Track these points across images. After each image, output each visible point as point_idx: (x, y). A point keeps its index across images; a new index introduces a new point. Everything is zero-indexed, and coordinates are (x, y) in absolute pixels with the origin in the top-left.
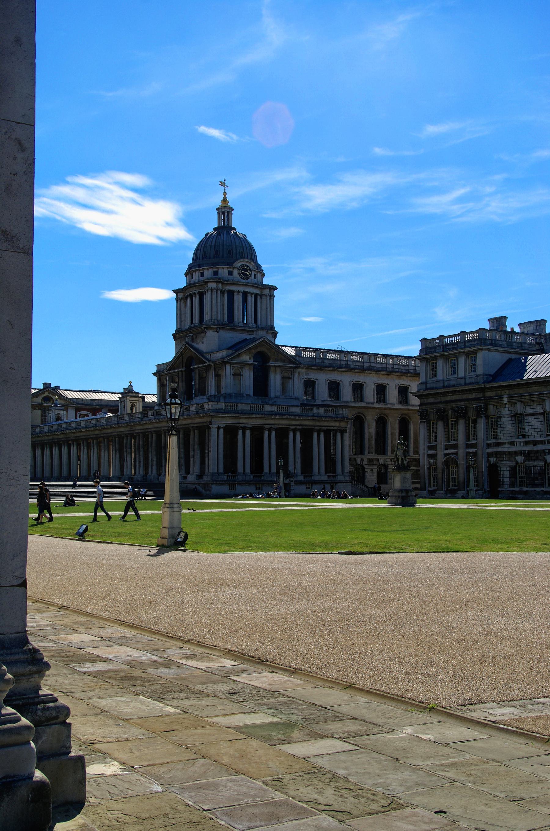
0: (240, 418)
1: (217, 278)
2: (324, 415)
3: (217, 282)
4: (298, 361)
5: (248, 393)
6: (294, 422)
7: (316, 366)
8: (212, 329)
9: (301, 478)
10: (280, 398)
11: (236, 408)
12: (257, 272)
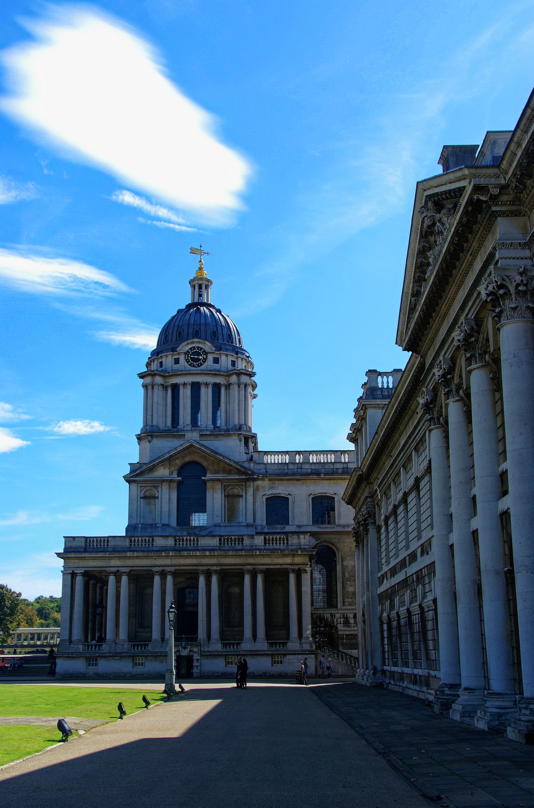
0: (110, 558)
4: (250, 470)
5: (167, 522)
7: (287, 474)
9: (218, 647)
10: (219, 526)
11: (106, 544)
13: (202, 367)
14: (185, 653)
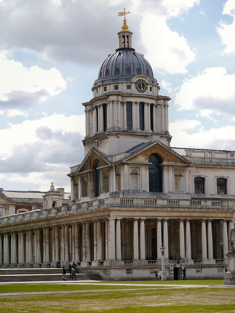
0: (135, 211)
1: (117, 92)
2: (211, 207)
3: (118, 95)
6: (183, 214)
7: (205, 165)
8: (114, 135)
9: (192, 262)
10: (173, 193)
12: (153, 86)
13: (145, 93)
14: (178, 266)
